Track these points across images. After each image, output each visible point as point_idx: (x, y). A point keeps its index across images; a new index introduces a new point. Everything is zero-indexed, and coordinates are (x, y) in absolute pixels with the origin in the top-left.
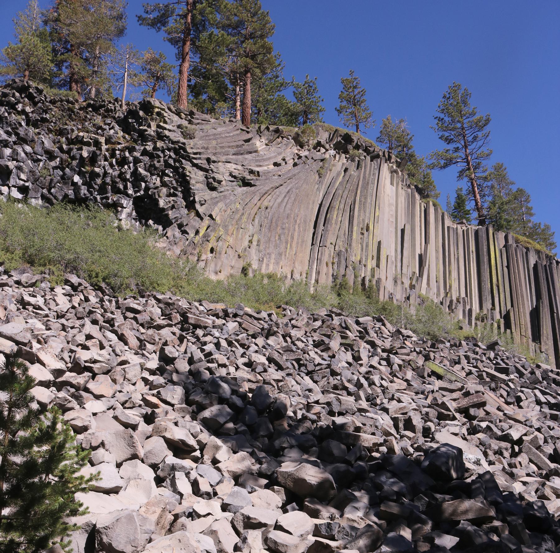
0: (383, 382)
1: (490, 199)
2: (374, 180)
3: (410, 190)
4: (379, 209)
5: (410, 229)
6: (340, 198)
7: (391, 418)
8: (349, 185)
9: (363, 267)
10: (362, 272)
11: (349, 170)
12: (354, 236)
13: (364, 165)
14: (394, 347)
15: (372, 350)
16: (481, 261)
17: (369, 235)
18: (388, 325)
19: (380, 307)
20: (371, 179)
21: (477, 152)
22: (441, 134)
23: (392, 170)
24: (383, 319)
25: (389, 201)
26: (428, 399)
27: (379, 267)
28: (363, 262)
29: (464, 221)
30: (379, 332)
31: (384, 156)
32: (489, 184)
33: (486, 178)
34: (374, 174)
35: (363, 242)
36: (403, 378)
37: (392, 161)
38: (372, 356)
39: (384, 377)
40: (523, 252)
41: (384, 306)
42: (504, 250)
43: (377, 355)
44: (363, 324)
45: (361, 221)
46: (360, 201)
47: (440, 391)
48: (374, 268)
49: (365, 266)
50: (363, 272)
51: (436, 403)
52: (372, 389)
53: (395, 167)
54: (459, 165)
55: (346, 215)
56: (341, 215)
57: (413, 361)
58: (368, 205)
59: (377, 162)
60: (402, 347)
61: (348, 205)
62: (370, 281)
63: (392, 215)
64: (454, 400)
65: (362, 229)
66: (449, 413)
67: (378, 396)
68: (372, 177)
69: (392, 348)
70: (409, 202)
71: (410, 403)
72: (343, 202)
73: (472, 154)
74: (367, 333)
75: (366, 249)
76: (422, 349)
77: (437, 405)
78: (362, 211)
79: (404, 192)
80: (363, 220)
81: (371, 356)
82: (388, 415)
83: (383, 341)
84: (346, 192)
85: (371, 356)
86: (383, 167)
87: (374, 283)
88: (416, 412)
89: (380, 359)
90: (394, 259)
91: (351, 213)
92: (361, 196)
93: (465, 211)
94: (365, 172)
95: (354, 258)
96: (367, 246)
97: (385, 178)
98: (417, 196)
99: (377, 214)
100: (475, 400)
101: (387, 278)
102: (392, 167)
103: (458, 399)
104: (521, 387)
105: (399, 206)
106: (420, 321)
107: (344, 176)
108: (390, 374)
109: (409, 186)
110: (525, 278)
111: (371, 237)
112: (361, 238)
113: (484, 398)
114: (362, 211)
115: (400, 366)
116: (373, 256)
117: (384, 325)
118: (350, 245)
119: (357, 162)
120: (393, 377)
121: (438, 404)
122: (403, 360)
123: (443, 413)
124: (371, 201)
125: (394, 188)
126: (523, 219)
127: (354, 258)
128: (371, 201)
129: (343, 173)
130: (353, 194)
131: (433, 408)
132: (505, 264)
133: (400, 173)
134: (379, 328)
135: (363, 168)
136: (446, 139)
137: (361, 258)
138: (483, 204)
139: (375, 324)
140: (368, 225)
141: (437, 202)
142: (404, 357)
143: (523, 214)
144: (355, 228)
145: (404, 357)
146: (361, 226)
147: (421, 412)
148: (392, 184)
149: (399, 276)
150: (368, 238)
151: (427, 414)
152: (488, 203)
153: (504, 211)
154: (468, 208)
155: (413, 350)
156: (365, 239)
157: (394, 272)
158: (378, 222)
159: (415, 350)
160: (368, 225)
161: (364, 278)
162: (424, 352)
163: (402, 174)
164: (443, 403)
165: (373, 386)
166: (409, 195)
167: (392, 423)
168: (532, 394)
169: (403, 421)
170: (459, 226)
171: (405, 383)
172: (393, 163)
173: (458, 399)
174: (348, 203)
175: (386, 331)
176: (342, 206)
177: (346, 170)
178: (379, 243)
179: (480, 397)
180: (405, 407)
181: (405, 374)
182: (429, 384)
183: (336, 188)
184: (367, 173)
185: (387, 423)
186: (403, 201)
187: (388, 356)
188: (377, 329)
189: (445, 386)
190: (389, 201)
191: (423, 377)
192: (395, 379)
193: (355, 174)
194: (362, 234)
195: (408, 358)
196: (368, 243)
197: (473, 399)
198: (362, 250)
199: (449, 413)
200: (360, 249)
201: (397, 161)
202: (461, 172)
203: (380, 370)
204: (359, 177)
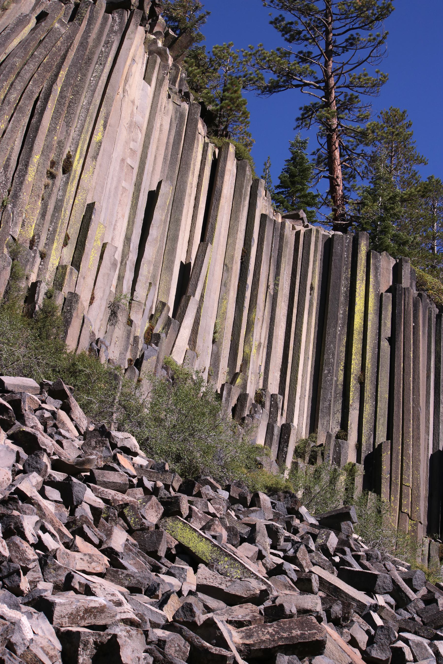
0: (47, 538)
1: (366, 184)
2: (107, 57)
3: (186, 106)
4: (105, 127)
5: (169, 201)
6: (13, 77)
7: (58, 632)
8: (41, 50)
9: (38, 260)
10: (31, 270)
11: (48, 19)
12: (30, 177)
13: (87, 16)
14: (89, 461)
15: (24, 456)
16: (330, 315)
17: (66, 183)
18: (78, 412)
19: (66, 364)
20: (98, 52)
21: (353, 73)
22: (276, 13)
23: (153, 48)
24: (68, 392)
25: (132, 113)
26: (165, 608)
27: (78, 268)
28: (41, 247)
29: (303, 214)
30: (51, 423)
31: (141, 7)
32: (369, 150)
33: (364, 134)
34: (107, 42)
35: (49, 196)
36: (101, 542)
37: (156, 29)
38: (24, 472)
39: (49, 527)
40: (430, 314)
41: (74, 364)
42: (388, 298)
43: (39, 471)
44: (12, 392)
45: (55, 143)
46: (62, 96)
47: (200, 595)
48: (64, 267)
49: (43, 256)
50: (36, 270)
51: (190, 619)
52: (12, 546)
53: (160, 44)
54: (306, 90)
55: (19, 121)
56: (7, 117)
57: (133, 508)
58: (79, 111)
59: (121, 17)
60: (107, 468)
61: (29, 97)
62: (49, 295)
63: (133, 152)
64: (238, 624)
65: (53, 164)
66: (224, 652)
67: (26, 570)
68: (101, 48)
69: (83, 463)
70: (178, 134)
71: (119, 604)
72: (19, 86)
73: (339, 75)
74: (21, 418)
75: (53, 216)
76: (160, 484)
77: (193, 626)
78: (61, 122)
79: (171, 106)
80: (61, 145)
81: (19, 472)
82: (51, 622)
83: (60, 443)
84: (32, 66)
85: (19, 472)
86: (134, 32)
87: (59, 301)
88: (134, 632)
89: (45, 483)
90: (118, 256)
91: (34, 120)
92: (65, 85)
93: (305, 196)
94: (88, 31)
95: (18, 229)
96: (58, 208)
97: (134, 60)
98: (201, 128)
99: (97, 137)
100: (296, 632)
101: (92, 298)
102: (155, 42)
103: (250, 623)
104: (401, 630)
105: (155, 134)
106: (159, 421)
107: (33, 30)
108: (67, 525)
109: (186, 97)
110: (428, 377)
111: (72, 188)
112: (46, 186)
113: (320, 631)
114: (61, 122)
115: (95, 510)
116: (67, 238)
117: (67, 408)
118: (16, 196)
119: (73, 6)
120: (73, 533)
121: (195, 623)
122: (106, 501)
123: (206, 650)
124: (90, 103)
125: (150, 90)
126: (433, 249)
127: (18, 229)
128: (90, 103)
129: (33, 21)
130: (48, 75)
131: (180, 632)
132: (387, 332)
133: (170, 61)
134: (54, 413)
135: (85, 22)
136: (285, 30)
137: (37, 235)
138: (347, 194)
139: (44, 402)
140: (69, 157)
141: (247, 153)
142: (111, 494)
143: (434, 239)
144: (36, 158)
145: (111, 494)
146: (52, 156)
147: (146, 633)
148: (147, 78)
149: (125, 302)
150: (65, 191)
151: (161, 643)
152: (360, 192)
153: (396, 216)
154: (311, 190)
155: (135, 481)
156: (55, 190)
157: (113, 289)
158: (95, 158)
159: (141, 484)
160: (69, 157)
161: (35, 285)
162: (163, 493)
163: (174, 65)
164: (210, 623)
165: (17, 539)
166: (182, 116)
167: (59, 646)
168: (431, 651)
169: (91, 645)
170: (289, 223)
171: (105, 560)
172: (158, 34)
173: (250, 623)
174: (32, 92)
175: (70, 425)
176: (14, 96)
177: (42, 17)
178: (90, 208)
179: (314, 628)
180: (101, 610)
181: (109, 534)
182: (169, 573)
183: (8, 51)
184: (93, 35)
185: (44, 643)
186: (166, 127)
187: (68, 479)
188: (47, 415)
189: (215, 584)
190: (132, 113)
191: (154, 554)
192: (79, 541)
193: (63, 31)
194: (52, 176)
195: (119, 496)
196: (62, 201)
197: (290, 629)
198: (43, 215)
199: (224, 652)
200: (38, 212)
201: (167, 34)
202: (307, 109)
203: (39, 507)
204: (70, 38)
